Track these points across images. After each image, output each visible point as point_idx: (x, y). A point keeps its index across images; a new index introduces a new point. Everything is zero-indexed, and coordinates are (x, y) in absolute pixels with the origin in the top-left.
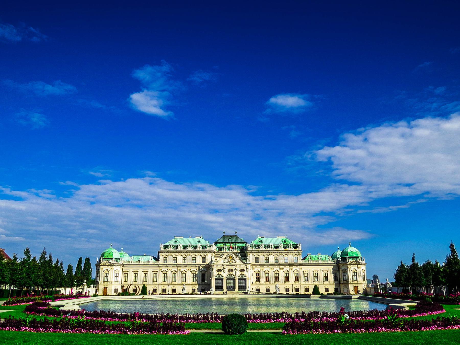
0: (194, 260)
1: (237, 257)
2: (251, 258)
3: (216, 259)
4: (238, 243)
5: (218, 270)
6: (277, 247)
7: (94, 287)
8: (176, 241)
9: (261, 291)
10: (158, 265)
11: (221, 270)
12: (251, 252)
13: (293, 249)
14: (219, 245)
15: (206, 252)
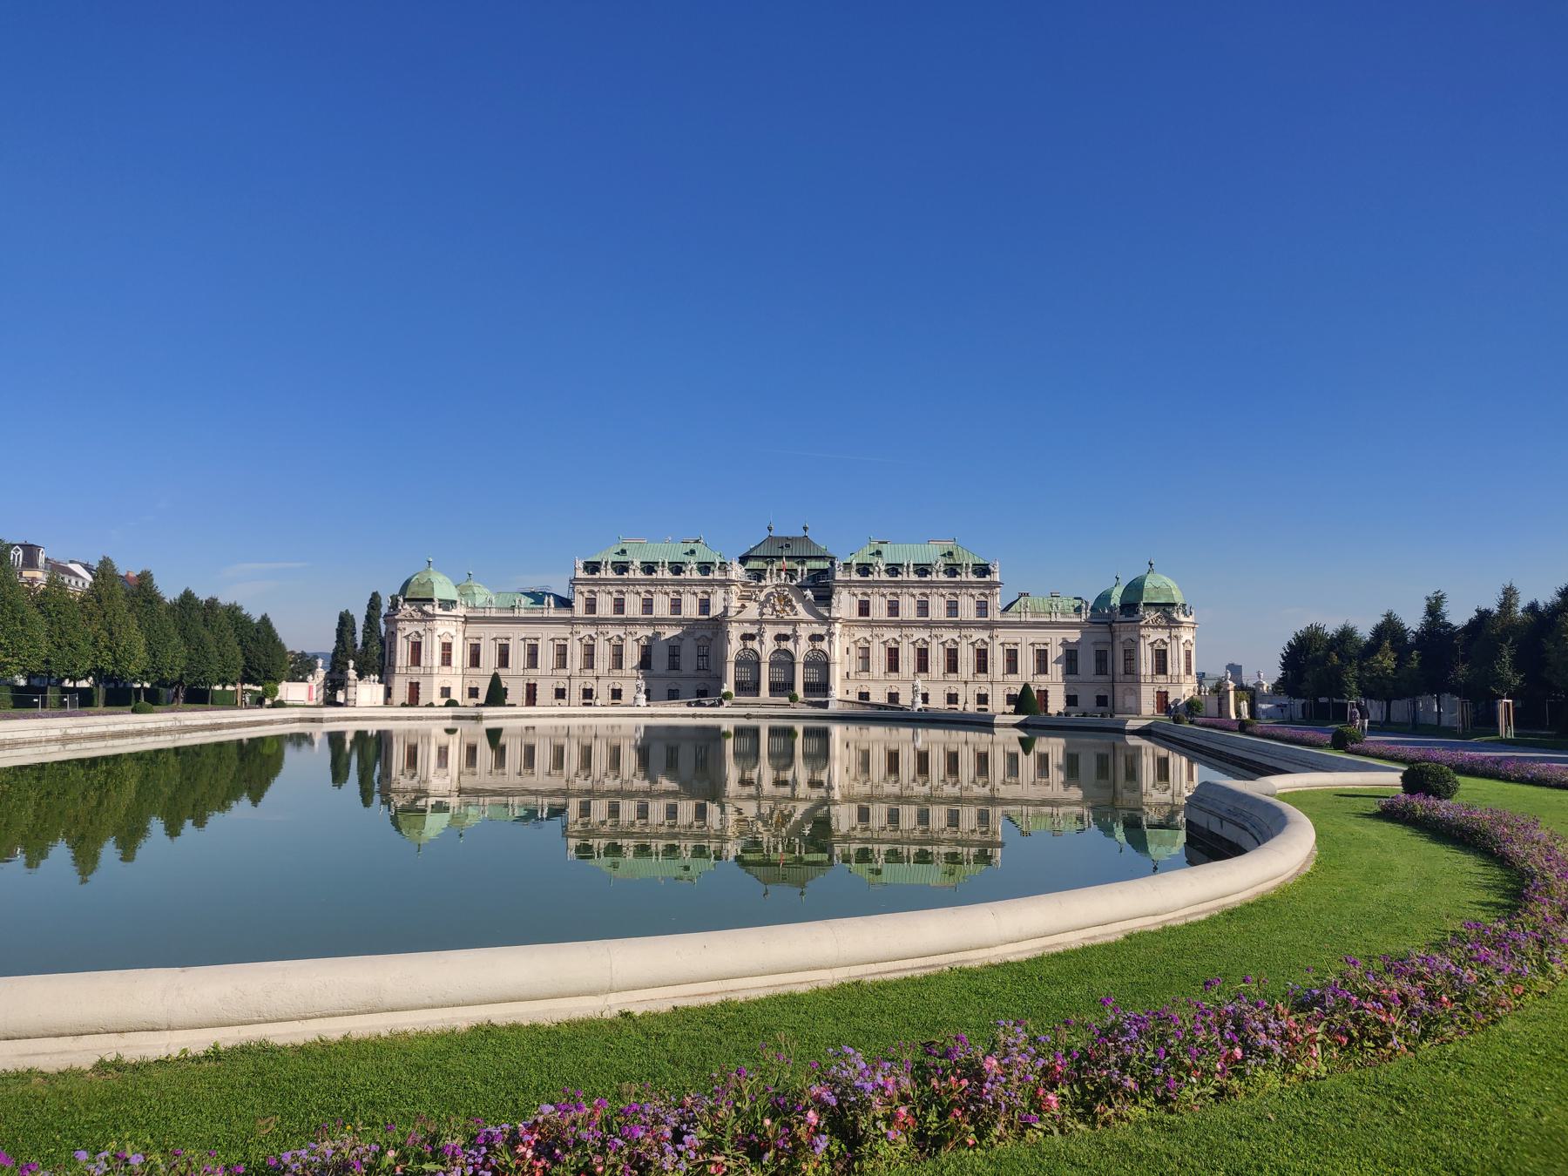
0: (676, 606)
1: (803, 599)
2: (844, 604)
3: (743, 606)
4: (810, 558)
5: (746, 637)
6: (923, 570)
7: (380, 682)
8: (624, 552)
9: (873, 699)
10: (570, 622)
11: (752, 637)
12: (848, 584)
13: (973, 578)
14: (752, 564)
15: (710, 583)
